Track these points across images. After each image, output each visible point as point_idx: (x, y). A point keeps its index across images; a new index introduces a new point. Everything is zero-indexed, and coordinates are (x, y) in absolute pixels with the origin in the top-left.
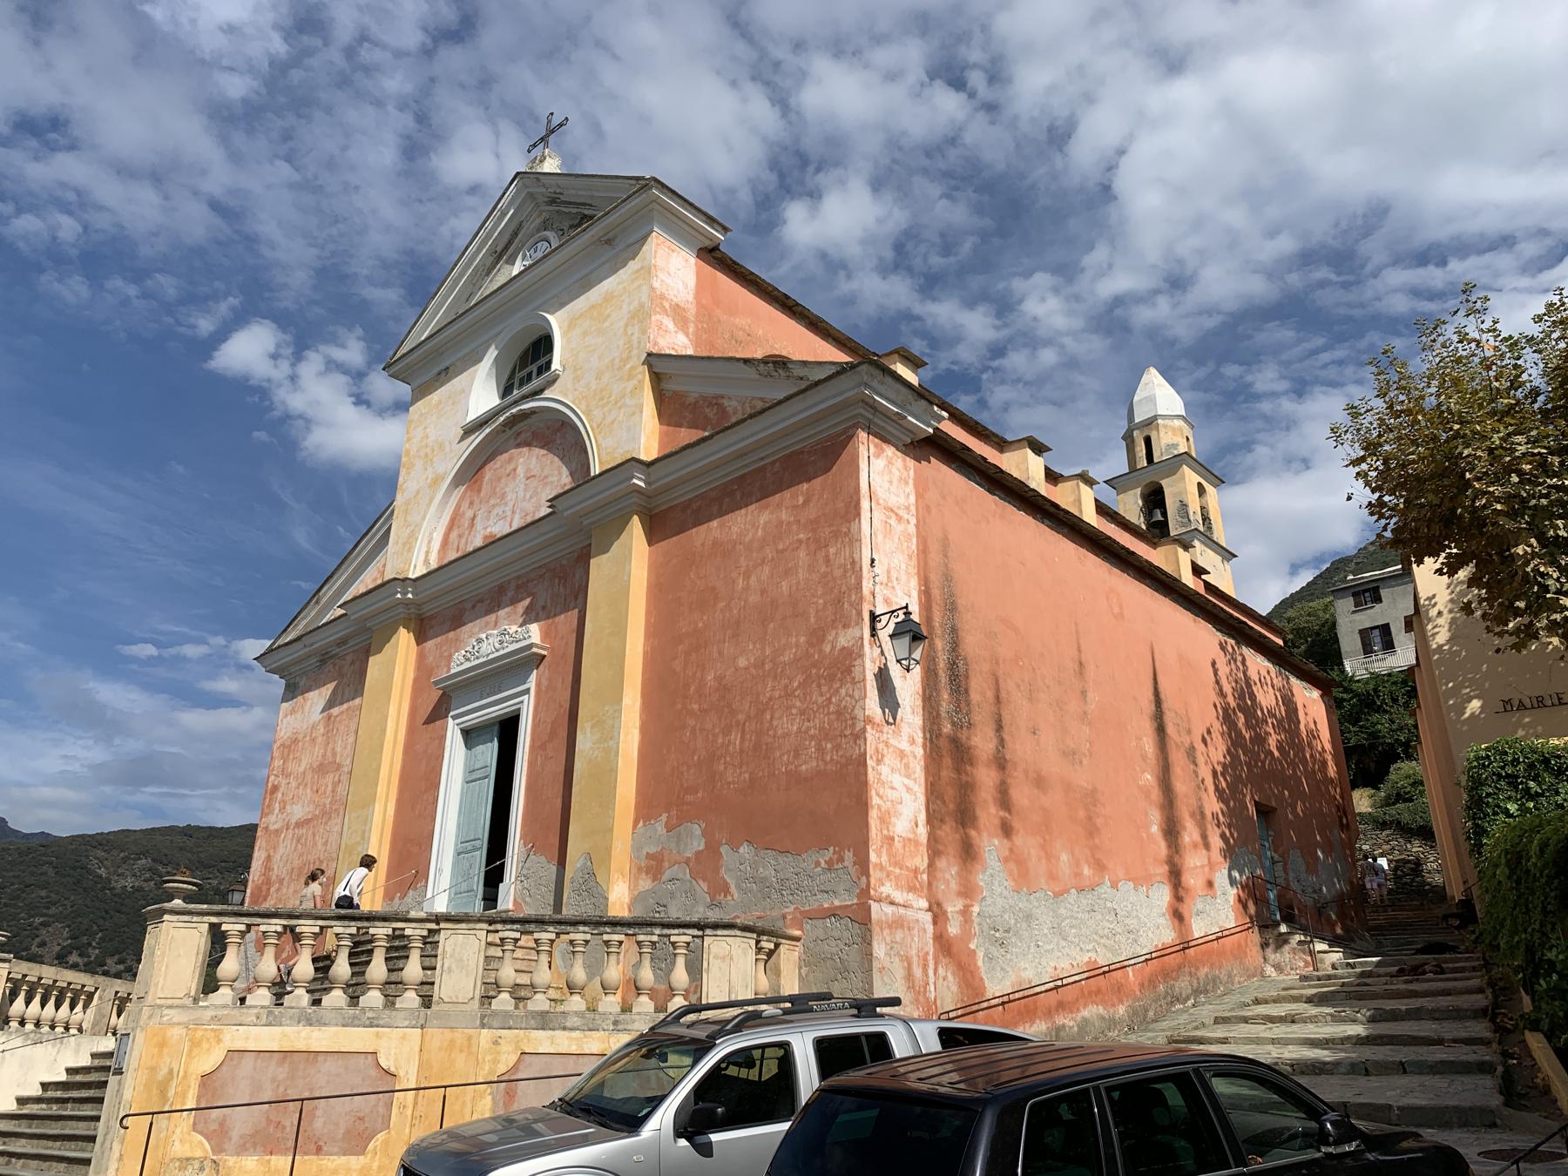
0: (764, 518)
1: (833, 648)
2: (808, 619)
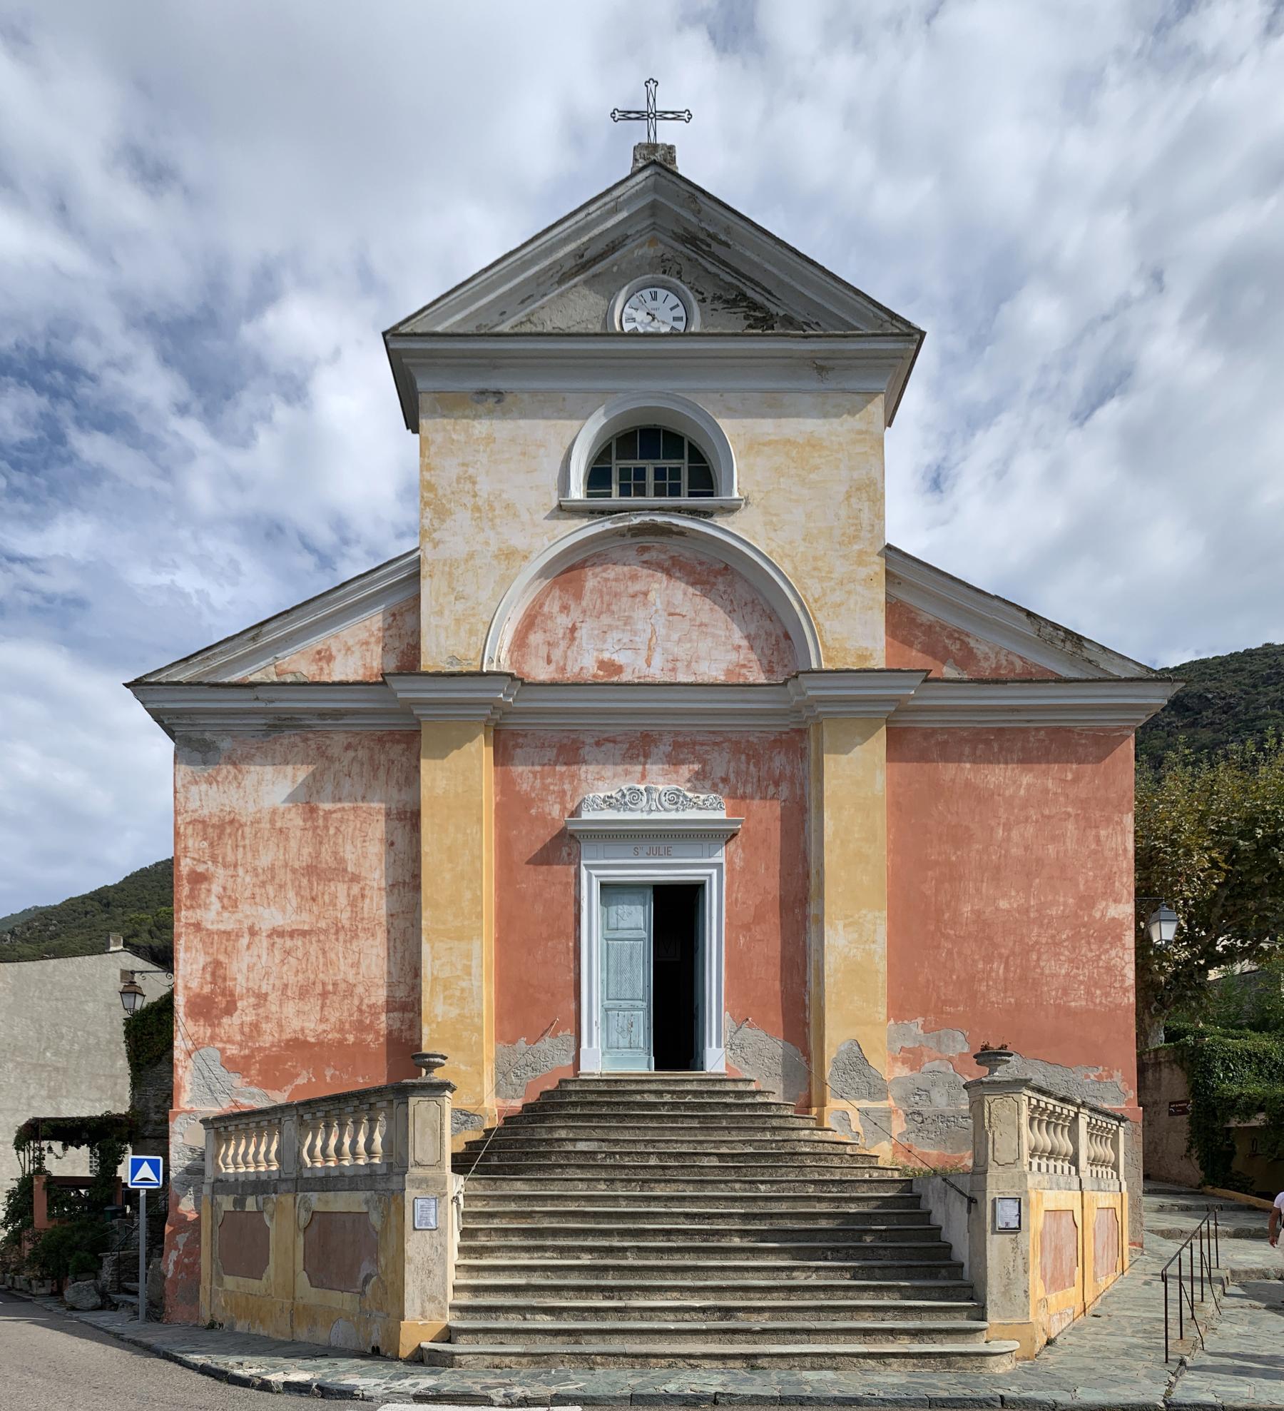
0: (1026, 779)
1: (1103, 915)
2: (1077, 885)
